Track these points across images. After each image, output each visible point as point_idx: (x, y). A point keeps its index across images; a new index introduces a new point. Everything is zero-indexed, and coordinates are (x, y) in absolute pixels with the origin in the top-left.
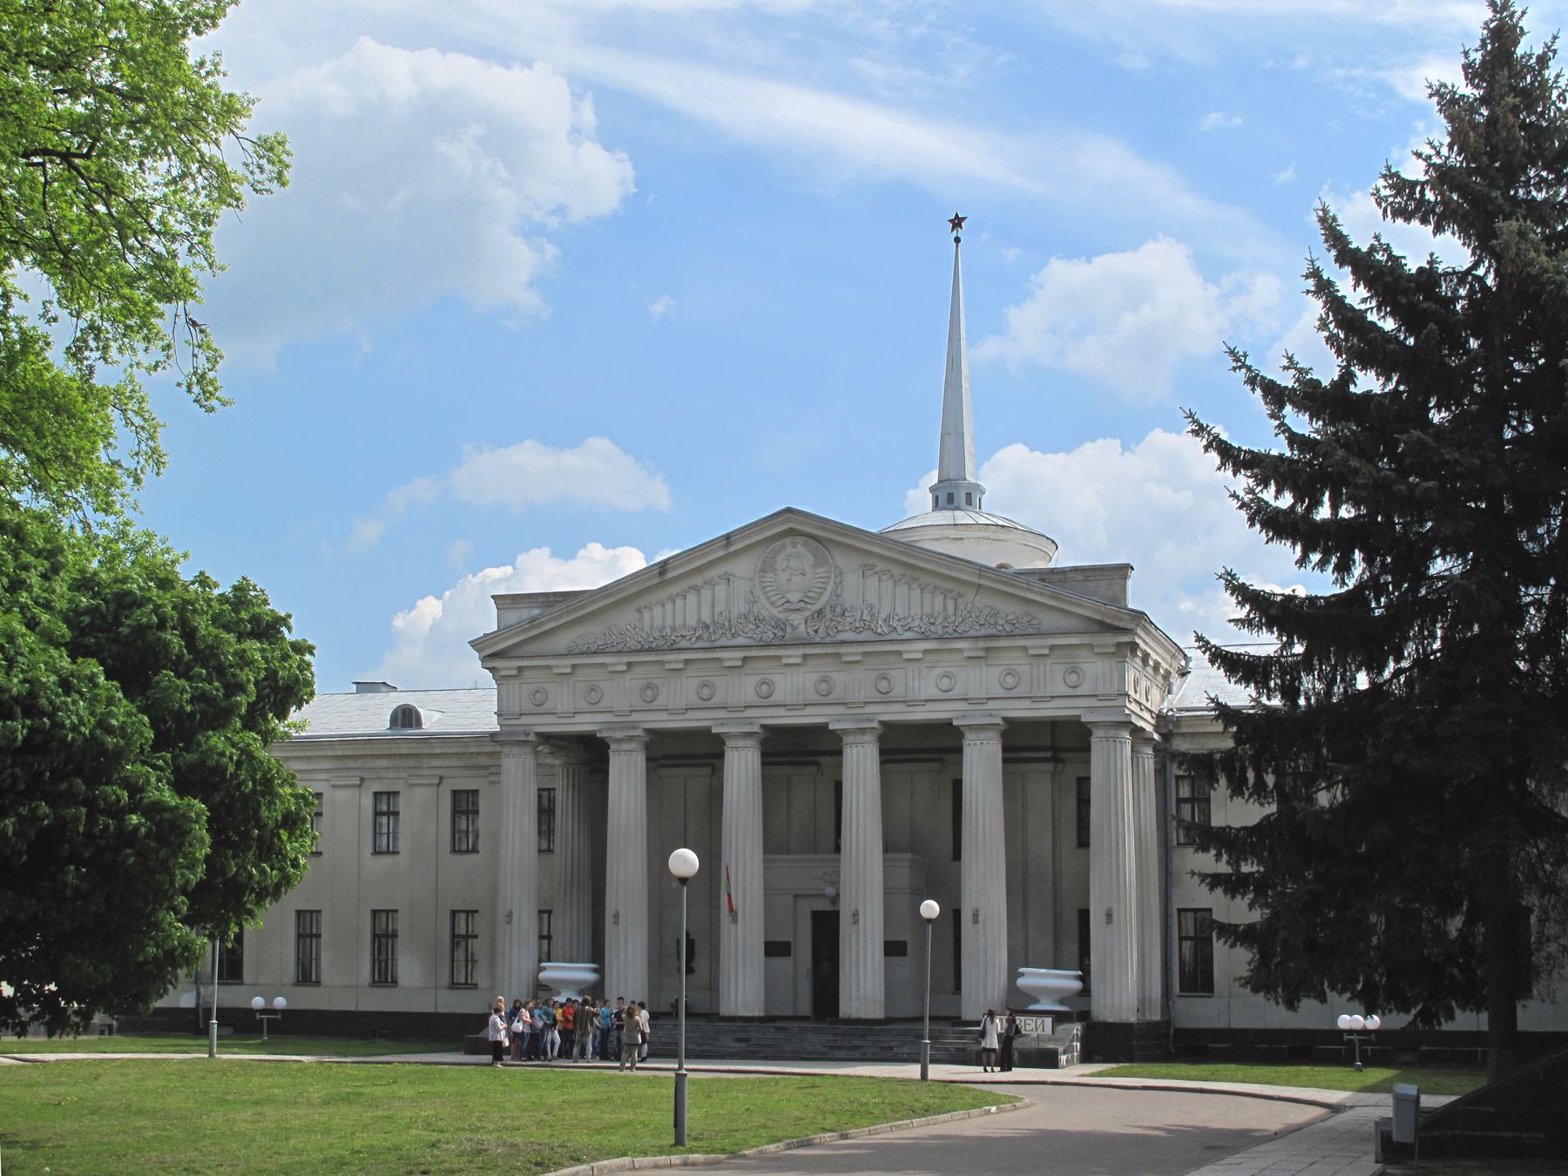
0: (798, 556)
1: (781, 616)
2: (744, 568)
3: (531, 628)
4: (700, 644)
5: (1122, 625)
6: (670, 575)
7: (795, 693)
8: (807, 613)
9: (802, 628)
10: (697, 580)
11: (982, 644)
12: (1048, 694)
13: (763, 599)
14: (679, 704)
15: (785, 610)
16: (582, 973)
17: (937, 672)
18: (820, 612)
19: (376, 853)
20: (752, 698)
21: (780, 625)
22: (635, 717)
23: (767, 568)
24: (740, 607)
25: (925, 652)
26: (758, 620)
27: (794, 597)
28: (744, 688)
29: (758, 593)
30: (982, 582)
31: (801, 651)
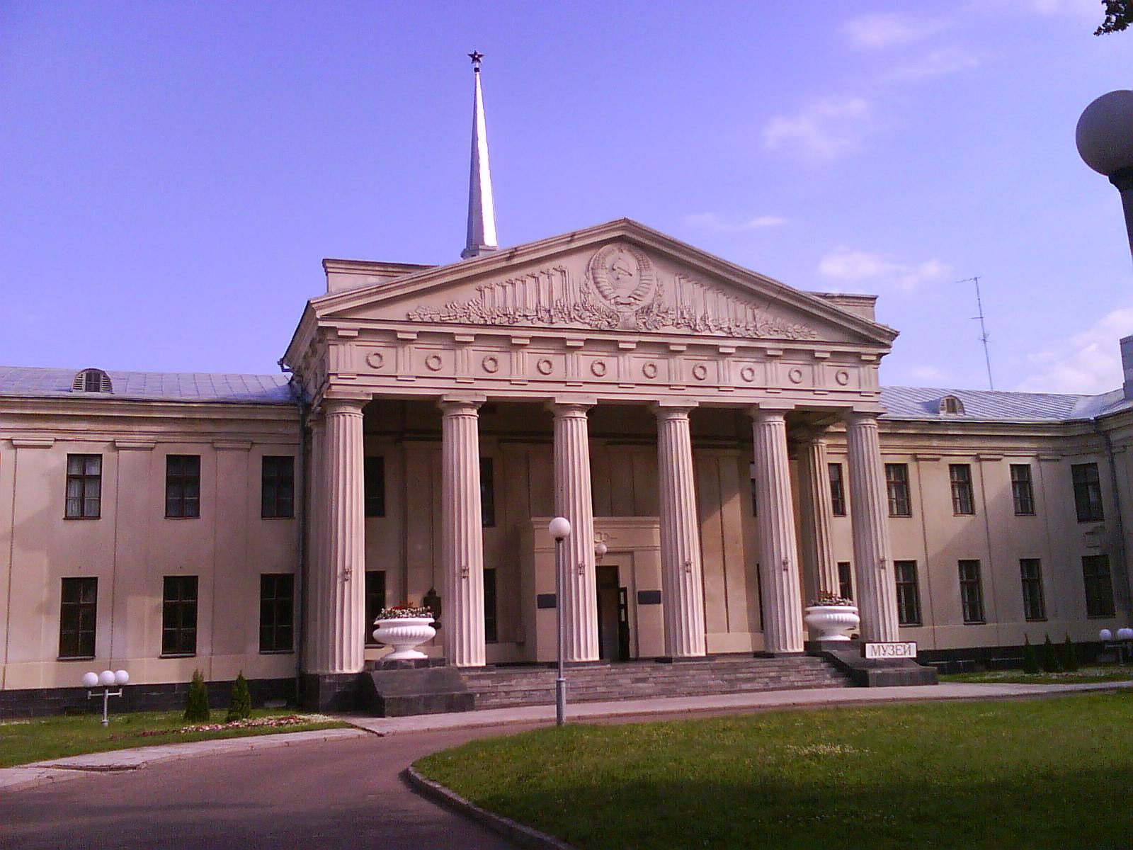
0: (627, 260)
1: (614, 307)
2: (575, 265)
3: (377, 293)
4: (540, 324)
5: (881, 340)
6: (516, 261)
7: (627, 377)
8: (635, 308)
9: (633, 319)
10: (535, 270)
11: (782, 346)
12: (825, 385)
13: (596, 291)
14: (520, 376)
15: (617, 303)
16: (422, 627)
17: (742, 365)
18: (647, 310)
19: (67, 518)
20: (585, 375)
21: (612, 315)
22: (477, 385)
23: (592, 270)
24: (575, 297)
25: (738, 348)
26: (594, 310)
27: (623, 294)
28: (581, 365)
29: (591, 283)
30: (780, 297)
31: (637, 338)
